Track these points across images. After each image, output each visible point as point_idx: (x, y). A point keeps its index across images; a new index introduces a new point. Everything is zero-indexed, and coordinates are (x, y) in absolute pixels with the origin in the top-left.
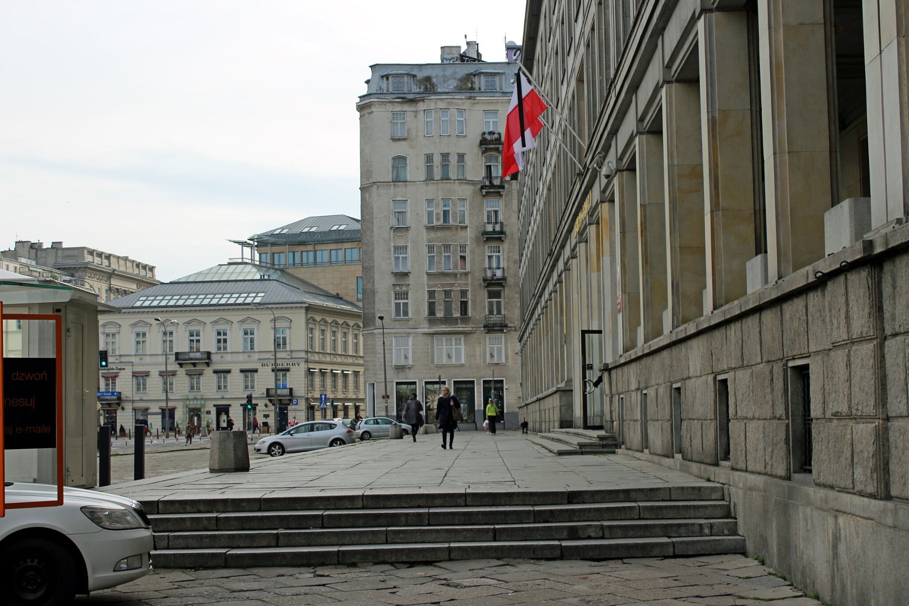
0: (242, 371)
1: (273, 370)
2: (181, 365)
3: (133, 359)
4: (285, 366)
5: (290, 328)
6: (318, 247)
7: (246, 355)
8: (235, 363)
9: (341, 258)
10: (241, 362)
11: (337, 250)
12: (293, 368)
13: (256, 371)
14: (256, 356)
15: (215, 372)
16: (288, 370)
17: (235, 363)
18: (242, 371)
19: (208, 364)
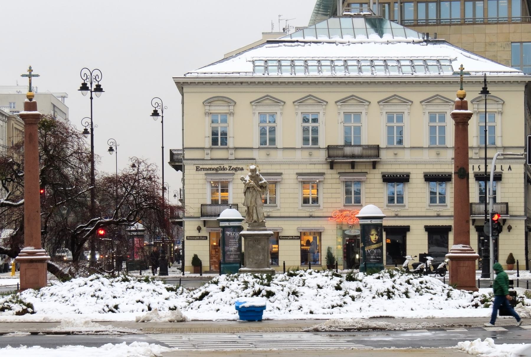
3: (255, 154)
5: (501, 113)
7: (433, 153)
8: (416, 163)
10: (425, 163)
17: (416, 163)
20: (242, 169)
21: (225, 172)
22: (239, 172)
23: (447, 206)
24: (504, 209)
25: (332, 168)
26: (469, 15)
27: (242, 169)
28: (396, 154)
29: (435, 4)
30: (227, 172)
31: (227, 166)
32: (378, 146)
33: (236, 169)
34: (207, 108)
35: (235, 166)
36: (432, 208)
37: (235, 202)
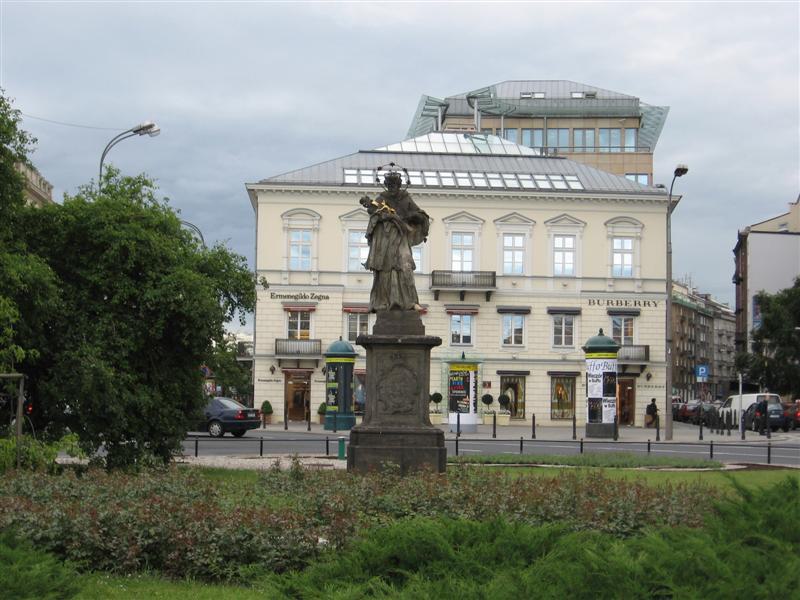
0: (552, 312)
1: (611, 313)
2: (437, 295)
3: (343, 280)
4: (631, 306)
6: (554, 124)
7: (559, 284)
9: (590, 142)
10: (549, 296)
11: (584, 129)
12: (645, 311)
13: (577, 312)
14: (579, 286)
15: (502, 311)
16: (637, 313)
18: (552, 312)
19: (488, 296)
20: (327, 298)
21: (307, 300)
22: (323, 301)
23: (574, 348)
24: (643, 353)
25: (436, 299)
26: (578, 142)
27: (327, 298)
28: (514, 284)
29: (541, 132)
30: (309, 300)
31: (308, 294)
32: (494, 273)
33: (319, 298)
34: (286, 222)
35: (318, 294)
36: (556, 350)
37: (318, 337)
